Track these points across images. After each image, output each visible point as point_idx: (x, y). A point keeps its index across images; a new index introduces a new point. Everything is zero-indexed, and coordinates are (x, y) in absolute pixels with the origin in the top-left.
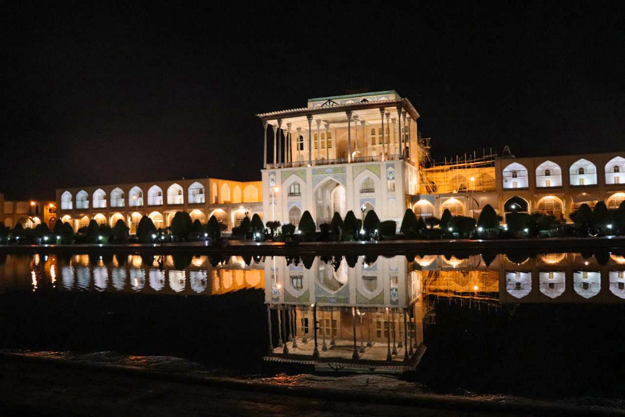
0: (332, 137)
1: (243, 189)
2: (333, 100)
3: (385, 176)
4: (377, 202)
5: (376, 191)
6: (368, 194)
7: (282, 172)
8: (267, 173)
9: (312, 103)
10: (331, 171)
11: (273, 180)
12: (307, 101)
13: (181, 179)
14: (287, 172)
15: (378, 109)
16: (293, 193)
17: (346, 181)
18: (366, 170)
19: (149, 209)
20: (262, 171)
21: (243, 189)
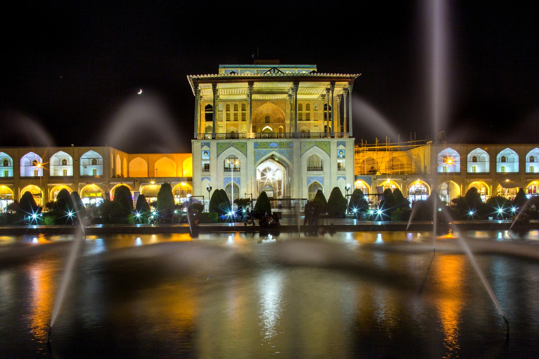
0: (246, 109)
1: (129, 162)
2: (280, 69)
3: (336, 154)
4: (326, 182)
5: (325, 168)
6: (315, 173)
7: (218, 144)
8: (200, 144)
9: (224, 69)
10: (276, 145)
11: (206, 152)
12: (218, 68)
13: (71, 146)
14: (224, 143)
15: (329, 83)
16: (227, 168)
17: (292, 158)
18: (315, 147)
19: (23, 181)
20: (192, 141)
21: (129, 162)
